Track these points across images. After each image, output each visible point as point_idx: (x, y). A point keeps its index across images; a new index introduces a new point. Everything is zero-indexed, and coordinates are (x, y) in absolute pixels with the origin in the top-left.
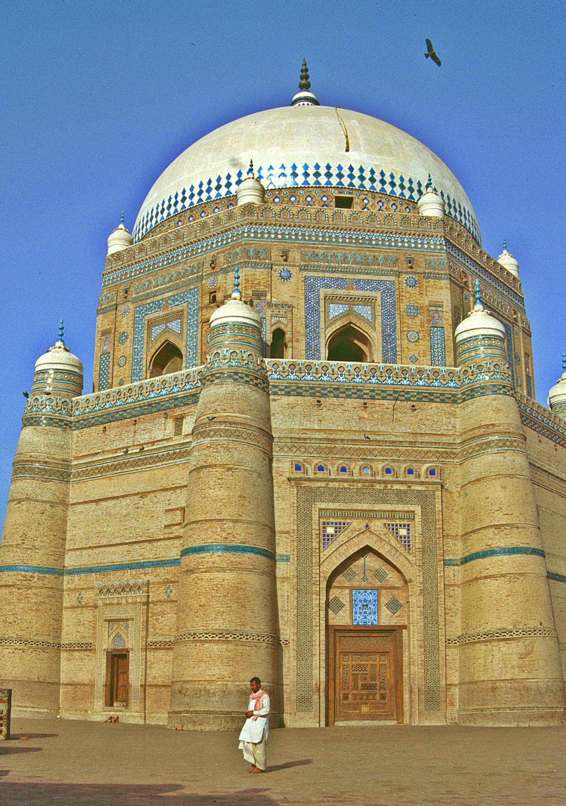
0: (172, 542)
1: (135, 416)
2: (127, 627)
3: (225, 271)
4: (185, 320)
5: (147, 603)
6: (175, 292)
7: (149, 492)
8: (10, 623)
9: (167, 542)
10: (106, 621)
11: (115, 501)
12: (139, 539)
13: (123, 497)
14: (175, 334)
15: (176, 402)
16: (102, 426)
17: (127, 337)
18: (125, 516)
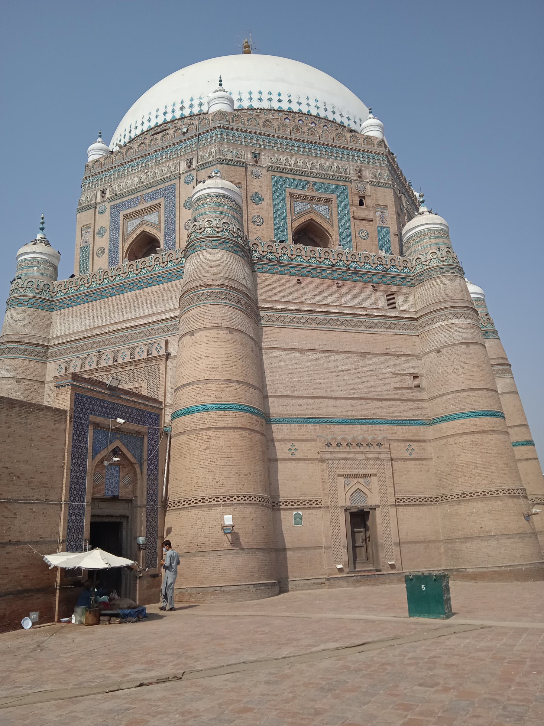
0: (404, 403)
1: (338, 279)
2: (368, 484)
3: (376, 184)
4: (335, 209)
5: (392, 459)
6: (322, 181)
7: (369, 353)
8: (245, 475)
9: (399, 403)
10: (339, 475)
11: (327, 355)
12: (365, 396)
13: (337, 352)
14: (323, 217)
15: (384, 279)
16: (295, 278)
17: (262, 200)
18: (343, 371)
